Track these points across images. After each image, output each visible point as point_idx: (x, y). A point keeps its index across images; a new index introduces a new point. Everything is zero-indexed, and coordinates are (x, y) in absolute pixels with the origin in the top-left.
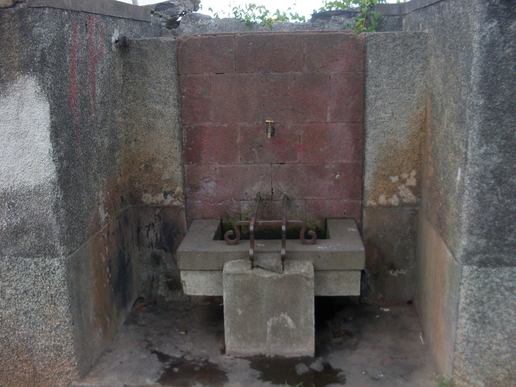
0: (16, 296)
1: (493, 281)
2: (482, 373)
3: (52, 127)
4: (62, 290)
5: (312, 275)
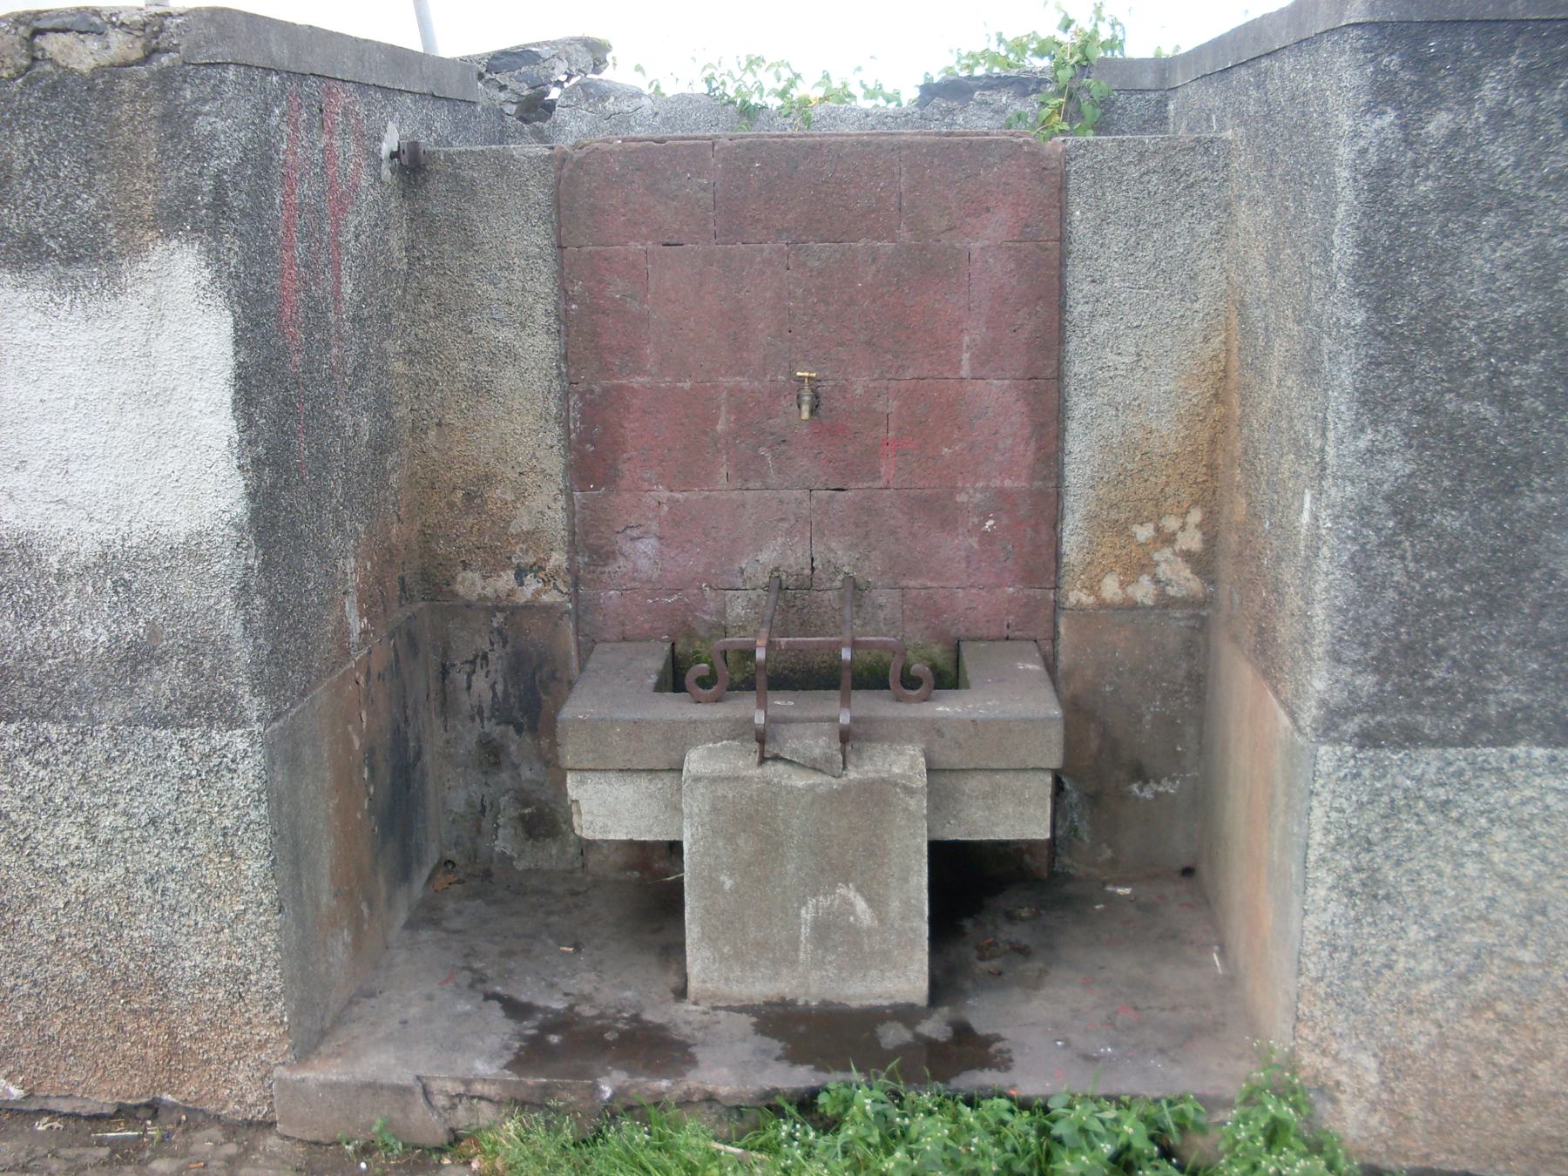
0: (127, 834)
1: (1395, 787)
2: (1370, 1034)
3: (238, 377)
4: (254, 815)
5: (921, 781)
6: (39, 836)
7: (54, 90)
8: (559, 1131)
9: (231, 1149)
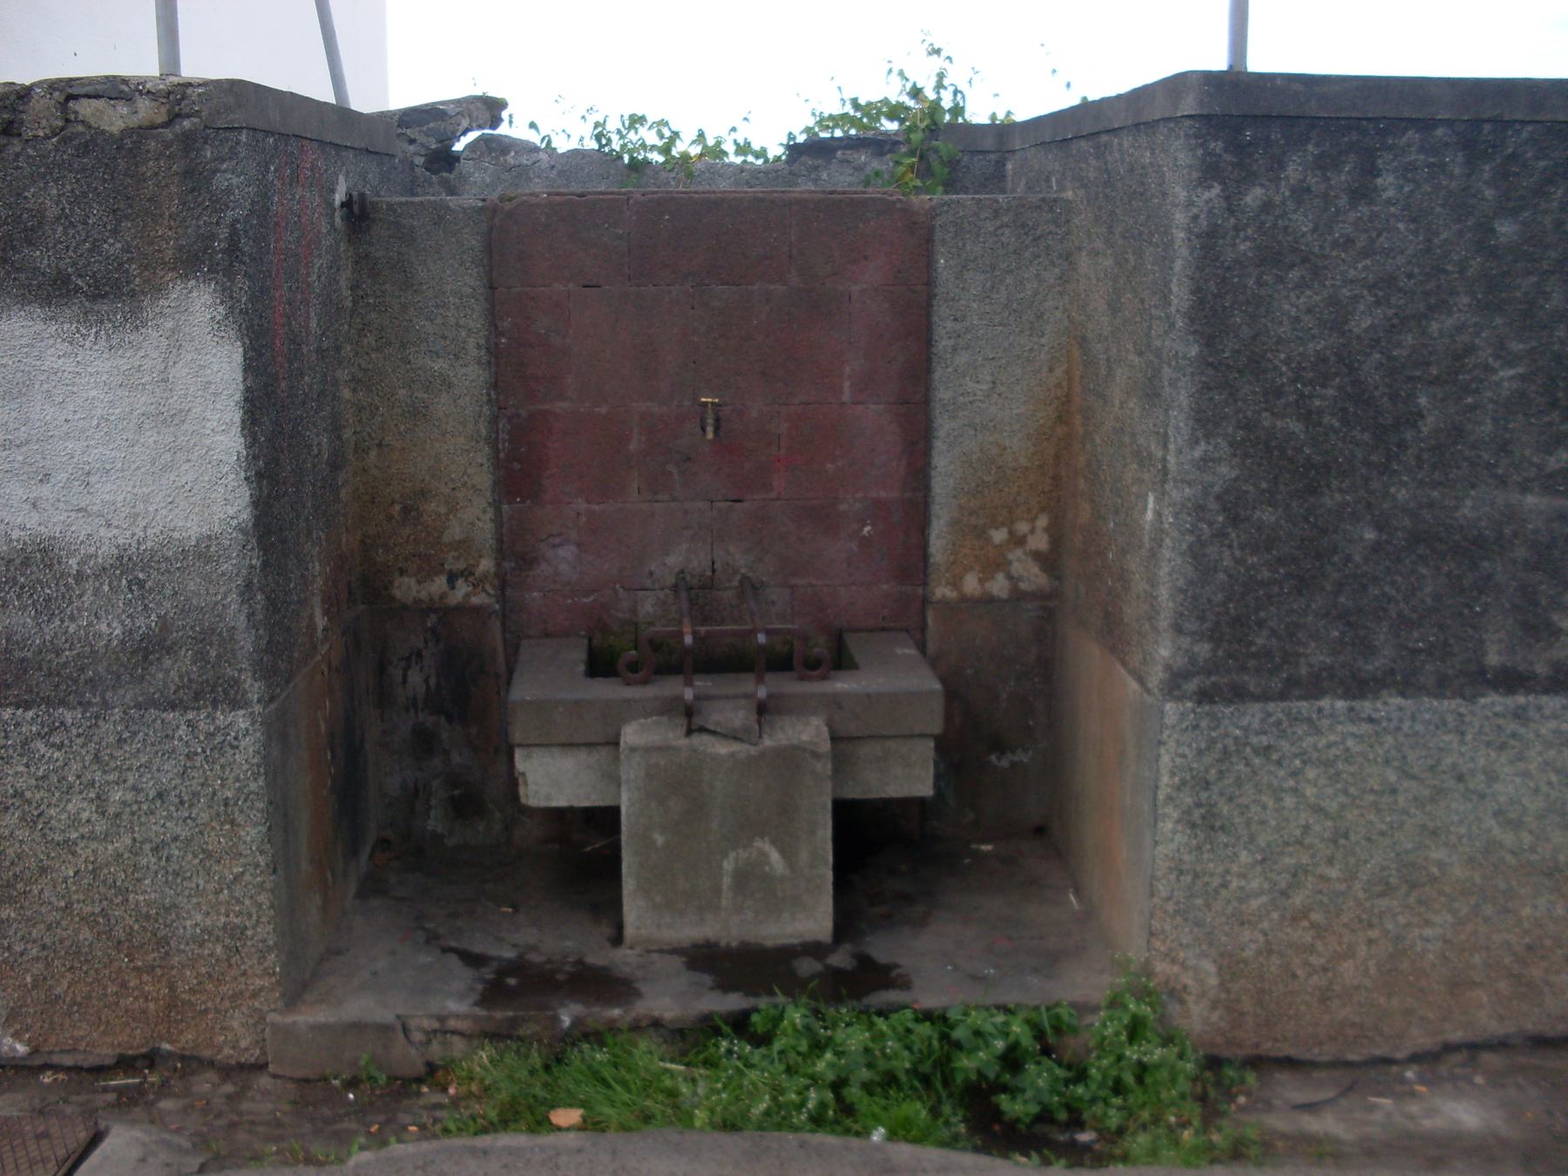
0: (135, 807)
1: (1227, 735)
2: (1210, 944)
3: (246, 400)
4: (253, 786)
5: (826, 746)
6: (52, 812)
7: (85, 148)
8: (527, 1057)
9: (229, 1088)
